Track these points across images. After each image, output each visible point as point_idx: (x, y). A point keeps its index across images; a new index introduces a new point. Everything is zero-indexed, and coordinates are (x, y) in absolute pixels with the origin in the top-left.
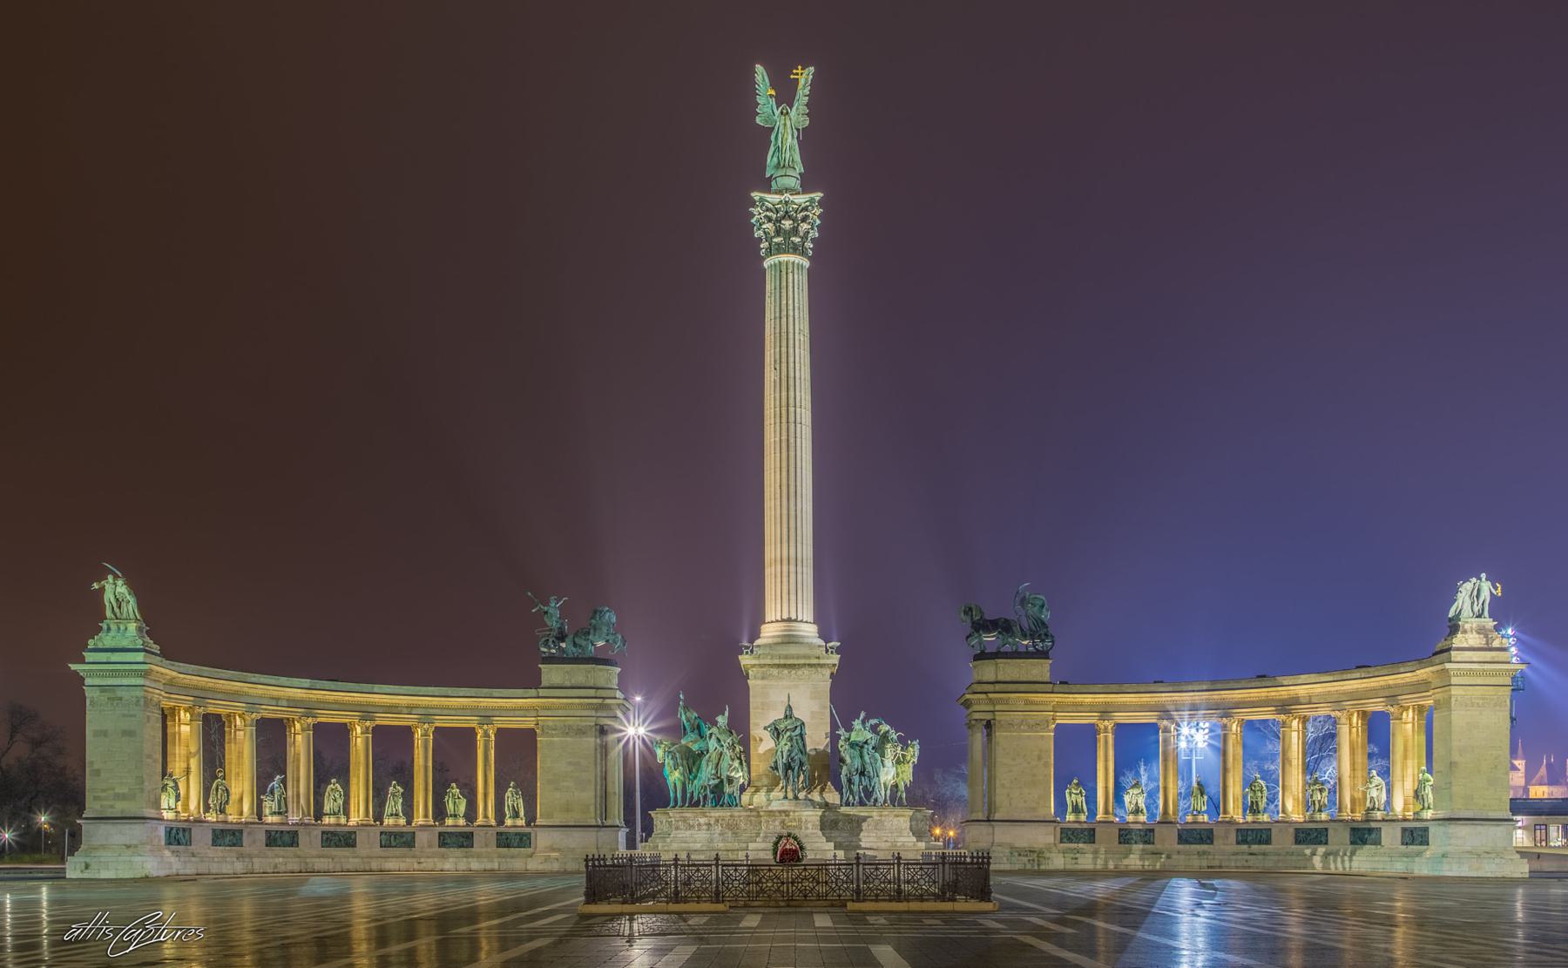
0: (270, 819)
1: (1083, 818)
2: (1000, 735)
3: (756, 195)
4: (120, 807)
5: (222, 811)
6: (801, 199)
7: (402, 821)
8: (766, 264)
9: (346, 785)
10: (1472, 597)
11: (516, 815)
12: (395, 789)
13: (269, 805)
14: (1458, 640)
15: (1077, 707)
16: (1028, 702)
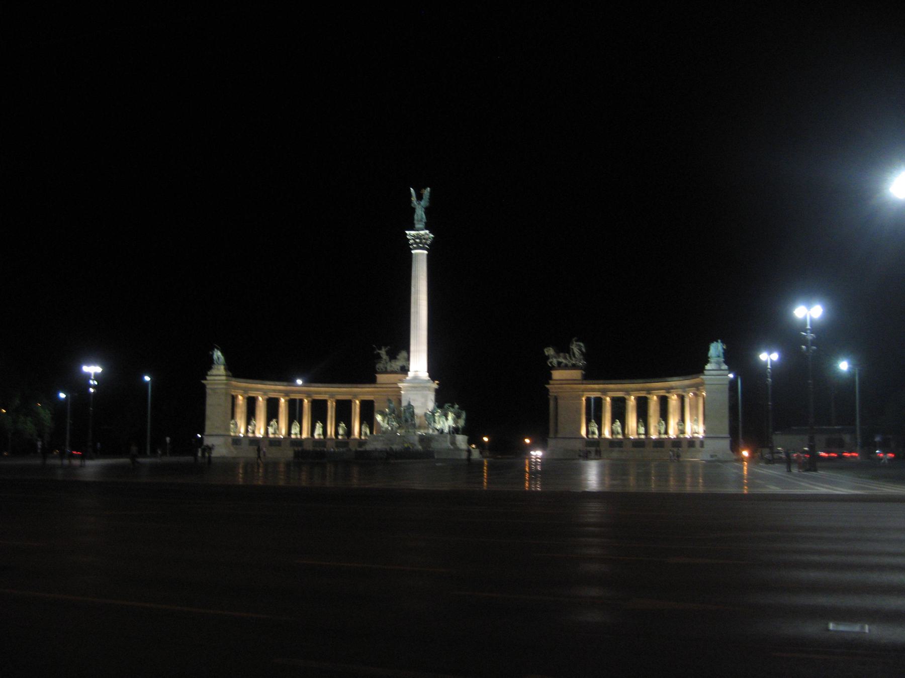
0: (271, 436)
1: (596, 436)
2: (560, 402)
3: (407, 232)
4: (216, 432)
5: (254, 432)
6: (422, 232)
7: (322, 437)
8: (413, 252)
9: (301, 423)
10: (716, 349)
11: (366, 434)
12: (319, 426)
13: (271, 430)
14: (708, 367)
15: (593, 390)
16: (572, 388)
